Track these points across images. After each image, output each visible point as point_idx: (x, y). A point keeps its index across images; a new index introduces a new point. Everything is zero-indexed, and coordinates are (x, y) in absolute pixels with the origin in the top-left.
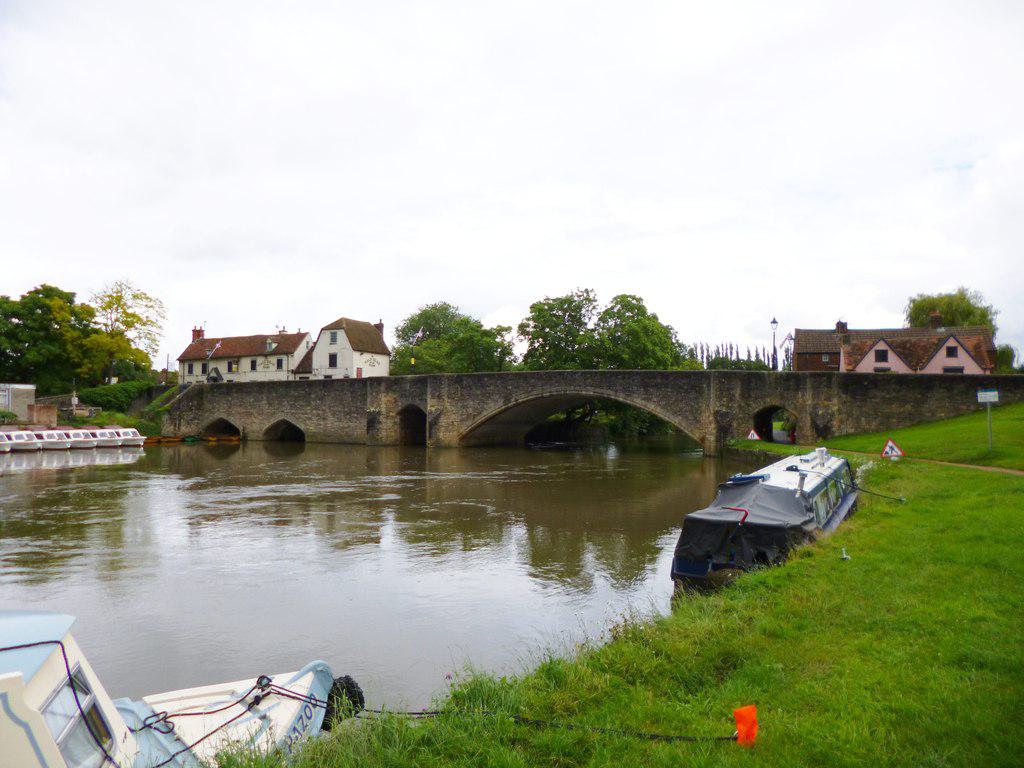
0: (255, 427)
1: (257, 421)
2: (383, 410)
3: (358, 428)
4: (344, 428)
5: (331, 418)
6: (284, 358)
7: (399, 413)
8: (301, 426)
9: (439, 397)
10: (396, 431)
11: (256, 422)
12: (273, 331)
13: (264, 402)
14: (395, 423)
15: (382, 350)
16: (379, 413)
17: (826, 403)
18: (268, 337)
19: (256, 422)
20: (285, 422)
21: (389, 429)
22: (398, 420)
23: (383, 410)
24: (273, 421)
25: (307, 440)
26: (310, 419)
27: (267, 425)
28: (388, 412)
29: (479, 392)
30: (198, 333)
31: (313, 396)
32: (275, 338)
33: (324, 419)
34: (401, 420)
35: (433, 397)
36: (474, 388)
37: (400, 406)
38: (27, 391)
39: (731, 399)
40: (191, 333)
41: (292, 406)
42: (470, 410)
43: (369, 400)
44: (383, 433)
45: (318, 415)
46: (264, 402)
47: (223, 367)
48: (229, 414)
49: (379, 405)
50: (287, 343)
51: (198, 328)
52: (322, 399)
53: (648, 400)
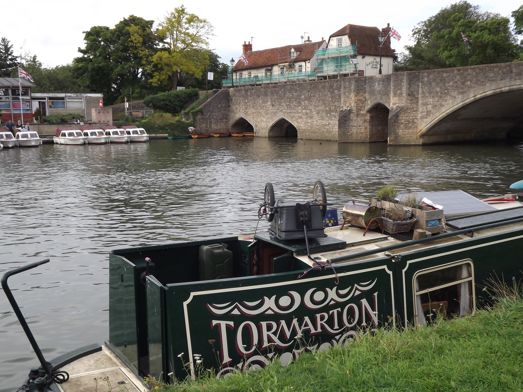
0: (264, 125)
1: (264, 119)
2: (354, 109)
3: (332, 126)
4: (325, 125)
5: (316, 116)
6: (303, 64)
7: (370, 111)
8: (295, 124)
9: (401, 94)
10: (366, 128)
11: (262, 121)
12: (299, 42)
13: (269, 103)
14: (365, 121)
15: (391, 54)
16: (350, 111)
18: (289, 48)
19: (262, 121)
21: (361, 128)
22: (368, 117)
23: (354, 109)
24: (276, 119)
25: (299, 136)
26: (301, 117)
27: (271, 123)
28: (359, 109)
29: (438, 89)
30: (247, 47)
31: (303, 97)
32: (298, 48)
33: (311, 117)
34: (371, 117)
35: (395, 95)
36: (434, 84)
37: (369, 105)
38: (98, 99)
40: (242, 47)
41: (289, 106)
42: (430, 107)
43: (342, 99)
44: (354, 130)
45: (307, 114)
46: (269, 103)
47: (261, 73)
48: (246, 114)
49: (350, 104)
50: (306, 51)
51: (247, 43)
52: (309, 99)
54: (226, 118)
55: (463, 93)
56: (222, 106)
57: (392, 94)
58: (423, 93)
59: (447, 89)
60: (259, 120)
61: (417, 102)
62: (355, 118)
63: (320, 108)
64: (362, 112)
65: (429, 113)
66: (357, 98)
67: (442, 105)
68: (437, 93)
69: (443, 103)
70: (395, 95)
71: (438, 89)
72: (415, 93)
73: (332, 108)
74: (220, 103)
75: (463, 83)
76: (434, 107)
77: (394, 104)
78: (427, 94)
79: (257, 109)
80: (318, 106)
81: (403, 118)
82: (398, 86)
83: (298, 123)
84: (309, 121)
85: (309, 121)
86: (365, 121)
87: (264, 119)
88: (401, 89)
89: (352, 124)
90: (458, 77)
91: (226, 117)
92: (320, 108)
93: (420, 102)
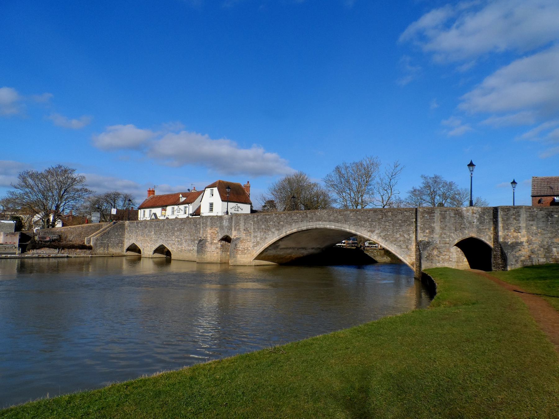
1: (149, 245)
9: (239, 229)
13: (153, 233)
17: (515, 234)
20: (162, 245)
24: (157, 245)
26: (174, 244)
28: (213, 239)
31: (176, 229)
33: (181, 244)
35: (235, 230)
36: (261, 223)
39: (432, 231)
42: (259, 238)
46: (153, 233)
49: (206, 235)
52: (180, 230)
53: (372, 232)
54: (122, 243)
55: (279, 230)
56: (118, 235)
57: (233, 229)
58: (254, 229)
59: (269, 227)
60: (145, 245)
61: (250, 235)
62: (209, 246)
63: (187, 237)
64: (214, 241)
65: (258, 243)
66: (211, 231)
67: (266, 238)
68: (263, 229)
69: (267, 236)
70: (235, 230)
71: (263, 227)
72: (248, 229)
73: (196, 238)
74: (117, 232)
75: (279, 223)
76: (261, 239)
77: (235, 236)
78: (257, 230)
79: (144, 237)
80: (186, 236)
81: (240, 246)
82: (237, 224)
83: (172, 248)
84: (180, 247)
85: (180, 247)
86: (217, 248)
87: (149, 245)
88: (238, 226)
89: (207, 250)
90: (275, 219)
91: (122, 242)
92: (187, 237)
93: (252, 235)
